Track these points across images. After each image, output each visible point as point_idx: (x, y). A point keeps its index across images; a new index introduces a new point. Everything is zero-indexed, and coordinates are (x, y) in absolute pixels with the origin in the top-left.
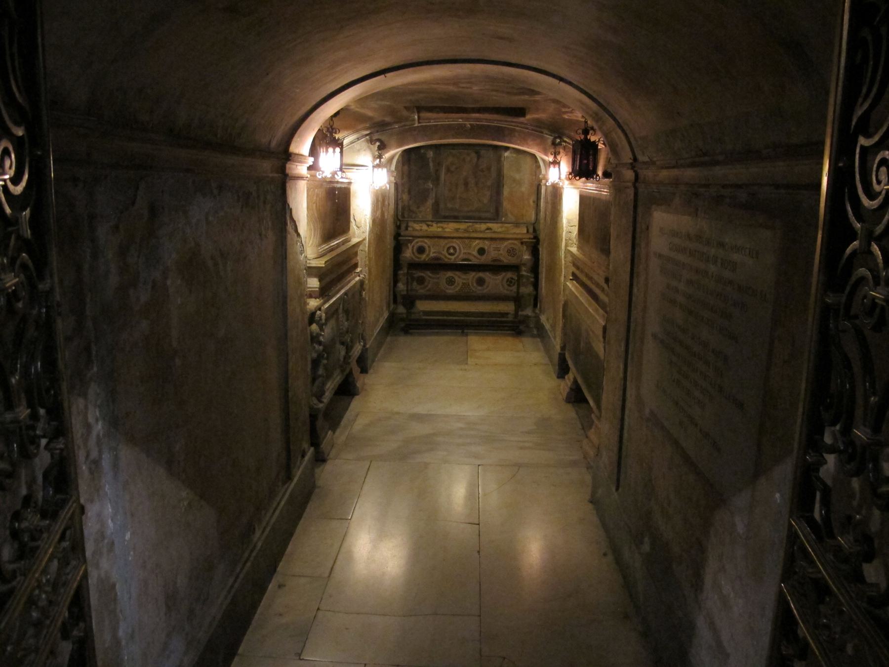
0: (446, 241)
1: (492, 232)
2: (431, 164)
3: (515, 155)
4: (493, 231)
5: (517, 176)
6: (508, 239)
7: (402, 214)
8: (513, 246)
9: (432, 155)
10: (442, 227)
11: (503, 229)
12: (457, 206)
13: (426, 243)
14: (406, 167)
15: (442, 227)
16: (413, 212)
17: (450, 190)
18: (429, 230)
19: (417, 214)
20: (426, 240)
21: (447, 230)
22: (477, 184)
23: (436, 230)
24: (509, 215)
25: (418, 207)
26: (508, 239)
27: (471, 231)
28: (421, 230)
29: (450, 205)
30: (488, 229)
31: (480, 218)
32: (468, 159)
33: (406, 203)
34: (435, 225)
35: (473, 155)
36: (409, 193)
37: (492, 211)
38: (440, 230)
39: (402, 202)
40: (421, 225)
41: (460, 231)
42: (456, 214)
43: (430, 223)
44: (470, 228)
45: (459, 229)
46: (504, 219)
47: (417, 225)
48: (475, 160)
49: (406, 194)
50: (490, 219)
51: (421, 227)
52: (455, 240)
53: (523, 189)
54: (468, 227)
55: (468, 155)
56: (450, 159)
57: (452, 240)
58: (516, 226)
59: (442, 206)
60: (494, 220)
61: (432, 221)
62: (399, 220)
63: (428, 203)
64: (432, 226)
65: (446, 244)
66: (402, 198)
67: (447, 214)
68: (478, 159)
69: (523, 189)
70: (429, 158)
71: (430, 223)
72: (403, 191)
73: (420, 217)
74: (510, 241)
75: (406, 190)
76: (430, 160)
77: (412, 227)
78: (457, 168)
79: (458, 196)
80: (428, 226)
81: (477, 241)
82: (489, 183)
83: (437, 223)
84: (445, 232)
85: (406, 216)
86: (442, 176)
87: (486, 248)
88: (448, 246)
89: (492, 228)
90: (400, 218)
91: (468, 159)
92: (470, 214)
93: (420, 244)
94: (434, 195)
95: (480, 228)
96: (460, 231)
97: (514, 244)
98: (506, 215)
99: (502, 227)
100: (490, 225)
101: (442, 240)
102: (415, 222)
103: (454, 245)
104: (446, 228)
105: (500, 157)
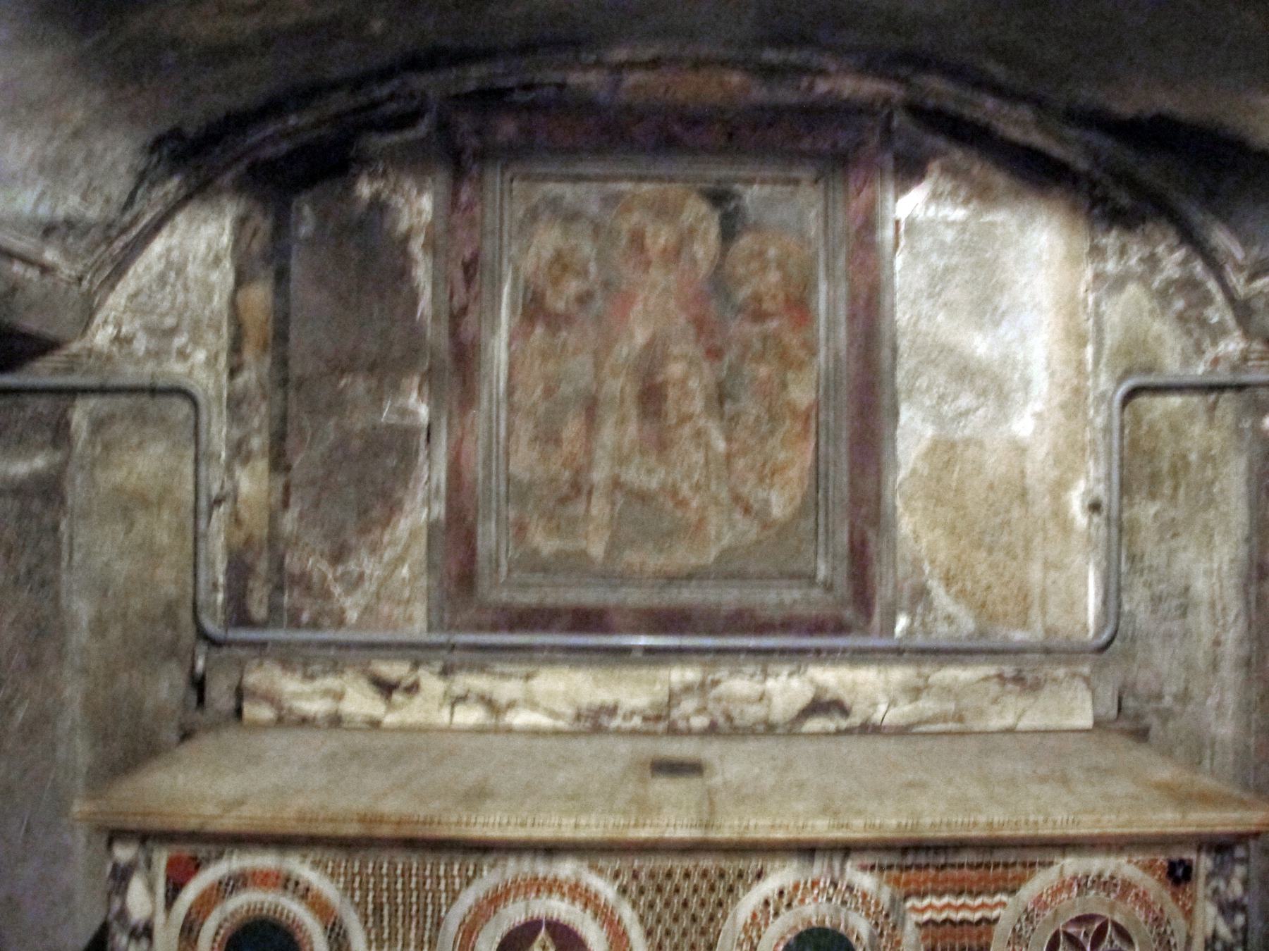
0: (491, 877)
1: (849, 731)
2: (422, 273)
3: (959, 214)
4: (855, 720)
5: (980, 345)
6: (1067, 845)
7: (228, 600)
8: (1095, 903)
9: (427, 215)
10: (488, 703)
11: (928, 705)
12: (597, 549)
13: (305, 894)
14: (259, 295)
15: (488, 703)
16: (303, 581)
17: (549, 437)
18: (390, 719)
19: (327, 595)
20: (301, 868)
21: (521, 718)
22: (721, 396)
23: (443, 717)
24: (942, 598)
25: (339, 555)
26: (1067, 845)
27: (699, 722)
28: (336, 721)
29: (545, 543)
30: (820, 706)
31: (743, 622)
32: (660, 237)
33: (256, 523)
34: (432, 684)
35: (697, 211)
36: (279, 462)
37: (822, 571)
38: (470, 716)
39: (236, 520)
40: (331, 682)
41: (616, 722)
42: (590, 597)
43: (394, 670)
44: (688, 705)
45: (612, 711)
46: (902, 622)
47: (307, 687)
48: (705, 249)
49: (262, 465)
50: (817, 628)
51: (339, 696)
52: (566, 868)
53: (1023, 426)
54: (673, 698)
55: (664, 211)
56: (548, 239)
57: (541, 868)
58: (1018, 679)
59: (488, 536)
60: (841, 628)
61: (416, 652)
62: (214, 643)
63: (404, 525)
64: (413, 689)
65: (496, 900)
66: (227, 497)
67: (529, 598)
68: (728, 233)
69: (1023, 426)
70: (407, 238)
71: (394, 670)
72: (239, 452)
73: (352, 616)
74: (1071, 865)
75: (257, 443)
76: (416, 247)
77: (271, 698)
78: (584, 299)
79: (600, 475)
80: (386, 688)
81: (782, 876)
82: (801, 394)
83: (446, 672)
84: (509, 730)
85: (259, 611)
86: (499, 349)
87: (860, 926)
88: (514, 914)
89: (847, 700)
90: (213, 626)
91: (660, 237)
92: (687, 596)
93: (241, 902)
94: (440, 474)
95: (762, 697)
96: (616, 722)
97: (1104, 884)
98: (921, 593)
99: (915, 692)
100: (831, 677)
101: (455, 867)
102: (289, 658)
103: (559, 908)
104: (511, 705)
105: (869, 224)
